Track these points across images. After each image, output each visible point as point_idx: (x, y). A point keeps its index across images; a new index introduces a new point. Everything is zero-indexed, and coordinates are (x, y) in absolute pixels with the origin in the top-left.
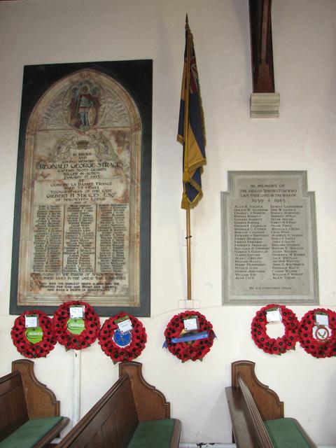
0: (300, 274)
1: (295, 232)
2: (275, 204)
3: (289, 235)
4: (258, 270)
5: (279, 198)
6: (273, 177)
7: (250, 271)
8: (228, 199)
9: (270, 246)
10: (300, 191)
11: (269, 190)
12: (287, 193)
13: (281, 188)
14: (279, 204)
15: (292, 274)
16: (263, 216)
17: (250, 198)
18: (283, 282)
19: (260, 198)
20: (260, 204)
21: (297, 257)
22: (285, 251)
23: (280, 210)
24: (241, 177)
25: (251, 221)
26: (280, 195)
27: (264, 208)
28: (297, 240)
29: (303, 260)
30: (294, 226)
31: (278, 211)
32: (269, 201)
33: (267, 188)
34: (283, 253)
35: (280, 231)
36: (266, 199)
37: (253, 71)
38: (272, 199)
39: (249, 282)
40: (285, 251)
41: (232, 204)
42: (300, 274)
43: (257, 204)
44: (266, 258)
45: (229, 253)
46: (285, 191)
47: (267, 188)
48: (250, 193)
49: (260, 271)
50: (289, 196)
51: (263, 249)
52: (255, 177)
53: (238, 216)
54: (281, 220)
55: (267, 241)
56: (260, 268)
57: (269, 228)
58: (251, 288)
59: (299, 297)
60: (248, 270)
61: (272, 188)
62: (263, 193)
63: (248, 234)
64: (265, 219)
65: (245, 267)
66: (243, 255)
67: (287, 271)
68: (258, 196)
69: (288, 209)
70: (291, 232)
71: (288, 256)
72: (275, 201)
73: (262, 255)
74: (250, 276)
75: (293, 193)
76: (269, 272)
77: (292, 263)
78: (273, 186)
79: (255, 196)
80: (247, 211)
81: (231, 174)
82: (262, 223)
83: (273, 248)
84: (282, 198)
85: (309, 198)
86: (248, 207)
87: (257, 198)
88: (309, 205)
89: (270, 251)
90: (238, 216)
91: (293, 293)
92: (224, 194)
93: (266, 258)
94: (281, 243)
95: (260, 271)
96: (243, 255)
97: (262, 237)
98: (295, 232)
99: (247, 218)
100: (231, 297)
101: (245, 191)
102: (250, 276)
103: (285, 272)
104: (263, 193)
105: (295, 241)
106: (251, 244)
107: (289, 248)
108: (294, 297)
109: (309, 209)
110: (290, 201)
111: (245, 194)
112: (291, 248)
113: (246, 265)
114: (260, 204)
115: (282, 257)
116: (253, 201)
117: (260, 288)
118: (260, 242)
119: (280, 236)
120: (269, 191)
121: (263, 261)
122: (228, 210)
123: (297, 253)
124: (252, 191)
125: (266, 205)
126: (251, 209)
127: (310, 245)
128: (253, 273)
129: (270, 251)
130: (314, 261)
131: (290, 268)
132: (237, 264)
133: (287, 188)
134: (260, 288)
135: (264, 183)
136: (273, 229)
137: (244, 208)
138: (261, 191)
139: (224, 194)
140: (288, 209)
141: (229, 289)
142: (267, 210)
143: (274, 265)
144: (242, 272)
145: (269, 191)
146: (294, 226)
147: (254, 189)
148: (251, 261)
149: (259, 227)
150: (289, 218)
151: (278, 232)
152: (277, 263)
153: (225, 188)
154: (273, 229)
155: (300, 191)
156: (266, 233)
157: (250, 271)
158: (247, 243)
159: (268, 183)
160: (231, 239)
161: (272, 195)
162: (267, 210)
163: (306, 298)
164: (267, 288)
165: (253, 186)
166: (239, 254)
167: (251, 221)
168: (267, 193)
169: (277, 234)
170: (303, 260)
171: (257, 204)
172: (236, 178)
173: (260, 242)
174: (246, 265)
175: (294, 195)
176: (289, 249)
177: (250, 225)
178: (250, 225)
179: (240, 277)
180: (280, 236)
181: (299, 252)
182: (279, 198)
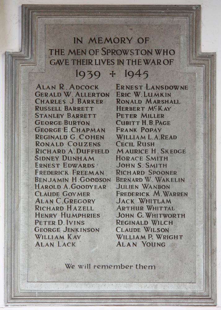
0: (176, 237)
1: (168, 145)
2: (125, 81)
3: (154, 151)
4: (85, 227)
5: (135, 69)
6: (122, 20)
7: (67, 229)
8: (23, 70)
9: (113, 176)
10: (182, 53)
11: (114, 50)
12: (155, 57)
13: (142, 46)
14: (135, 81)
15: (159, 237)
16: (98, 109)
17: (72, 69)
18: (136, 254)
19: (94, 68)
20: (92, 82)
21: (172, 198)
22: (145, 187)
23: (137, 94)
24: (52, 20)
25: (71, 120)
26: (138, 62)
27: (102, 90)
28: (173, 163)
29: (182, 205)
30: (165, 130)
31: (133, 97)
32: (113, 74)
33: (109, 46)
34: (141, 189)
35: (135, 143)
36: (105, 70)
37: (6, 205)
38: (120, 70)
39: (65, 254)
40: (145, 187)
41: (30, 81)
42: (176, 237)
43: (86, 81)
44: (103, 201)
45: (23, 191)
46: (148, 52)
47: (109, 46)
48: (71, 57)
49: (90, 230)
50: (159, 63)
51: (96, 180)
52: (83, 20)
53: (44, 109)
54: (139, 118)
55: (106, 164)
56: (90, 223)
57: (111, 134)
58: (68, 266)
59: (171, 288)
60: (63, 227)
61: (122, 46)
62: (100, 56)
63: (65, 147)
64: (103, 116)
65: (56, 220)
66: (52, 194)
67: (147, 230)
68: (90, 62)
69: (154, 92)
70: (159, 144)
71: (151, 197)
72: (127, 74)
73: (94, 194)
74: (66, 241)
75: (165, 57)
76: (109, 231)
77: (159, 212)
78: (122, 41)
79: (80, 62)
80: (63, 97)
81: (29, 13)
82: (95, 123)
83: (118, 179)
84: (143, 67)
85: (201, 69)
86: (67, 87)
87: (86, 68)
88: (200, 85)
89: (113, 186)
90: (44, 109)
91: (160, 278)
92: (12, 60)
93: (103, 201)
94: (136, 169)
95: (90, 230)
96: (52, 194)
97: (94, 155)
98: (168, 145)
99: (63, 111)
100: (24, 287)
101: (60, 52)
102: (66, 241)
103: (143, 233)
104: (100, 56)
105: (168, 163)
106: (70, 170)
107: (153, 178)
108: (161, 288)
109: (200, 94)
110: (160, 75)
111: (60, 57)
112: (158, 180)
113: (58, 217)
114: (92, 82)
115: (137, 200)
116: (78, 73)
117: (89, 266)
118: (89, 166)
119: (135, 151)
120: (113, 52)
121: (96, 207)
122: (22, 94)
123: (171, 190)
124: (76, 52)
125: (106, 84)
126: (73, 92)
127: (201, 174)
128: (73, 234)
129: (113, 186)
130: (206, 209)
131: (154, 223)
132: (40, 214)
133: (153, 45)
134: (89, 266)
135: (104, 35)
136: (120, 137)
137: (57, 90)
138: (96, 52)
139: (12, 60)
140: (154, 92)
141: (21, 269)
142: (107, 95)
143: (120, 215)
144: (49, 230)
145: (113, 52)
146: (165, 130)
147: (80, 46)
148: (69, 208)
149: (89, 133)
150: (156, 112)
151: (131, 144)
152: (125, 212)
153: (15, 44)
154: (120, 137)
155: (182, 53)
156: (103, 147)
157: (67, 229)
158: (61, 168)
159: (112, 35)
160: (28, 159)
161: (120, 62)
162: (107, 95)
163: (187, 289)
164: (104, 267)
165: (77, 40)
166: (43, 191)
167: (71, 120)
168: (110, 57)
169: (129, 148)
170: (182, 205)
171: (86, 81)
172: (40, 23)
173: (89, 166)
174: (58, 217)
175: (170, 62)
176: (153, 182)
177: (69, 127)
178: (69, 127)
179: (44, 242)
180: (135, 151)
181: (175, 187)
182: (135, 69)
